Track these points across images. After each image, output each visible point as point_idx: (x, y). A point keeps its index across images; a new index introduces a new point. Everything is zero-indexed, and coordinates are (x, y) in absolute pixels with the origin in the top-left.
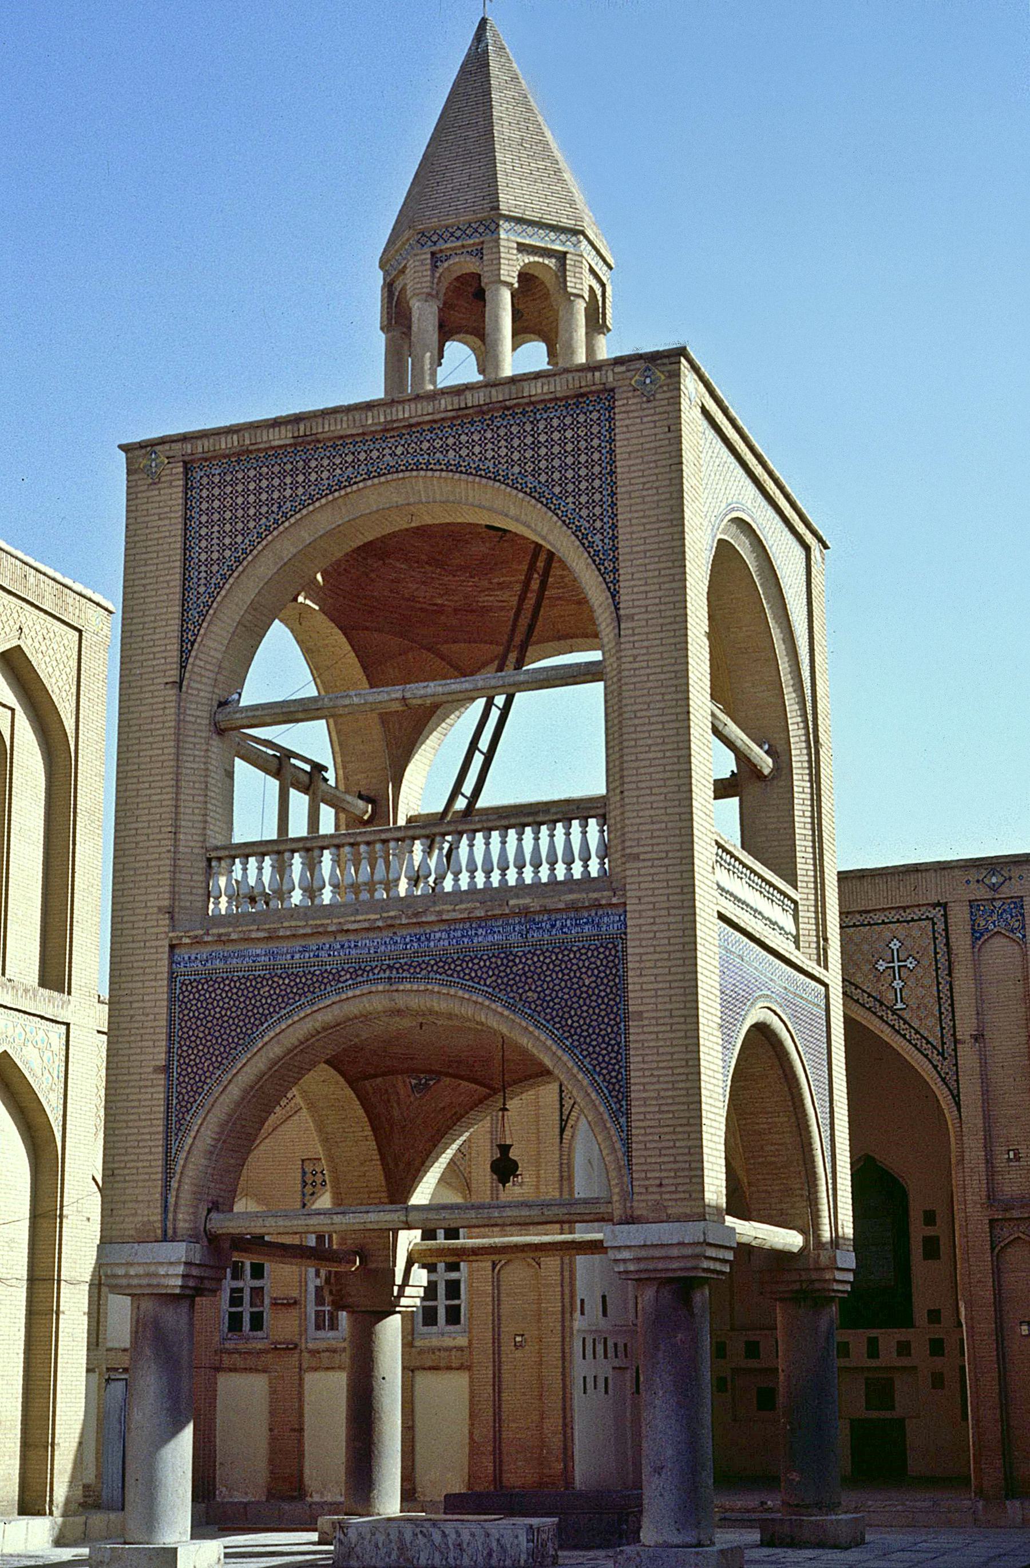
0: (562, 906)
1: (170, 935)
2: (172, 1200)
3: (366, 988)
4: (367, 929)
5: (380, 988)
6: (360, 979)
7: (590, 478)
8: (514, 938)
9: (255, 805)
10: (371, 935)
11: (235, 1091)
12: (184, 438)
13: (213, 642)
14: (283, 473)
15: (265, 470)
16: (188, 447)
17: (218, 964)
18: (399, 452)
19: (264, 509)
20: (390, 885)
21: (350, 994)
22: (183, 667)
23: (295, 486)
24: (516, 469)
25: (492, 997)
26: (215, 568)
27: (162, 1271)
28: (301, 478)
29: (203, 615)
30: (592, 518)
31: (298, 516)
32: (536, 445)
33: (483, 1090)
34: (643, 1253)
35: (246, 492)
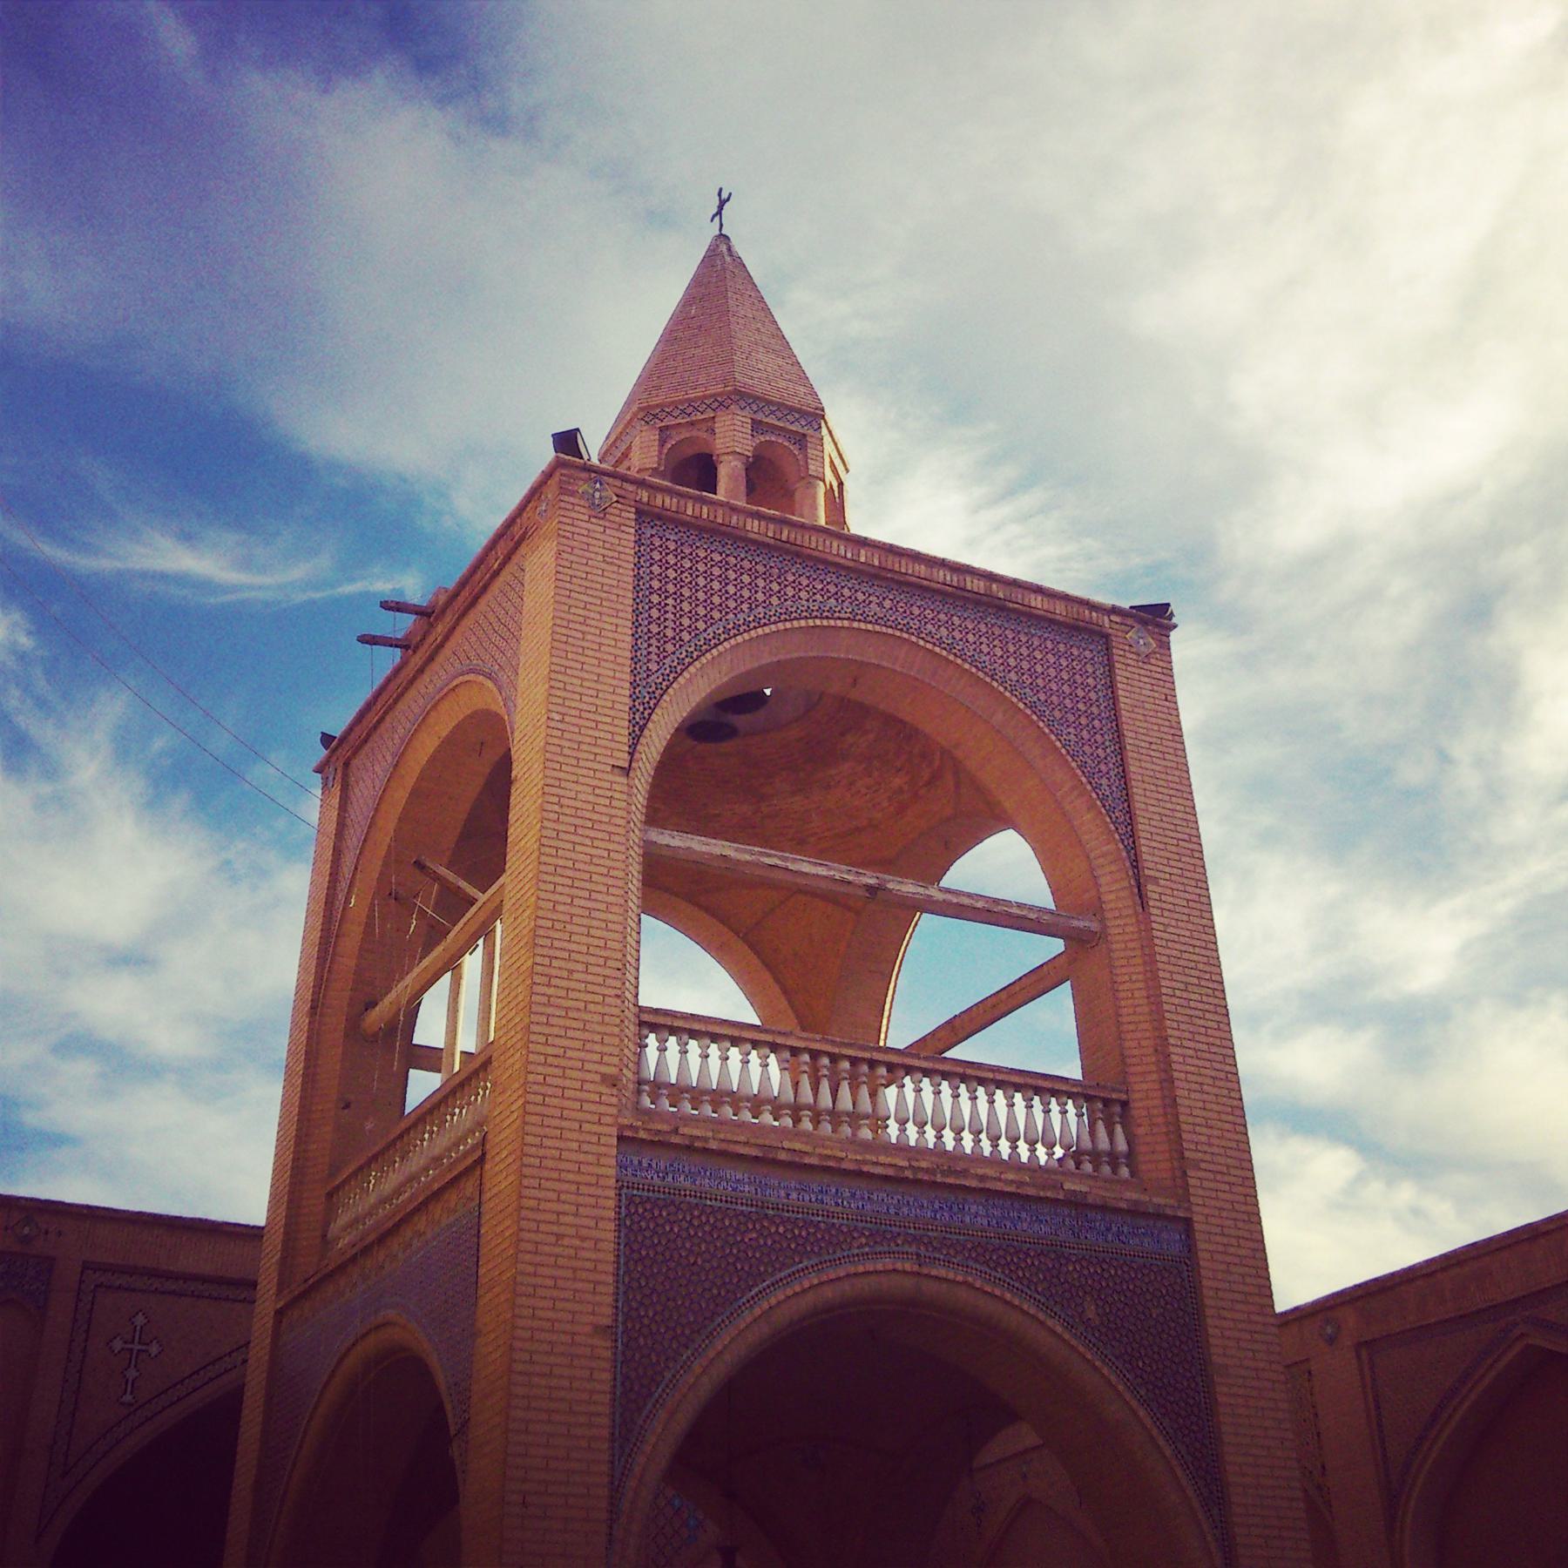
0: (1123, 1205)
1: (621, 1120)
4: (886, 1178)
5: (908, 1267)
6: (879, 1249)
10: (889, 1187)
15: (732, 560)
17: (683, 1182)
28: (775, 587)
31: (905, 636)
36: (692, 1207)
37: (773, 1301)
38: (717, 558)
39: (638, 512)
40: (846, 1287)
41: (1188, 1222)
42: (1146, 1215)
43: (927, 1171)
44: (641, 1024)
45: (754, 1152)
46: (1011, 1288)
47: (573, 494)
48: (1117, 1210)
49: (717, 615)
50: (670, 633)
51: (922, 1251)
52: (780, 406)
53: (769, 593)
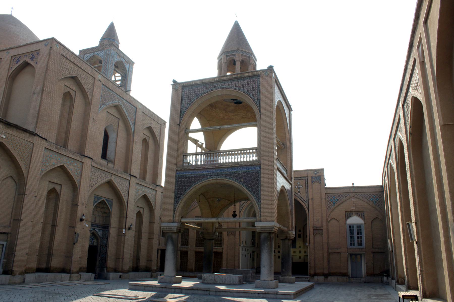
3: (212, 179)
7: (255, 90)
9: (191, 148)
11: (187, 196)
13: (186, 118)
14: (199, 89)
20: (218, 160)
22: (180, 122)
25: (235, 181)
29: (184, 113)
30: (256, 97)
35: (193, 92)
40: (206, 183)
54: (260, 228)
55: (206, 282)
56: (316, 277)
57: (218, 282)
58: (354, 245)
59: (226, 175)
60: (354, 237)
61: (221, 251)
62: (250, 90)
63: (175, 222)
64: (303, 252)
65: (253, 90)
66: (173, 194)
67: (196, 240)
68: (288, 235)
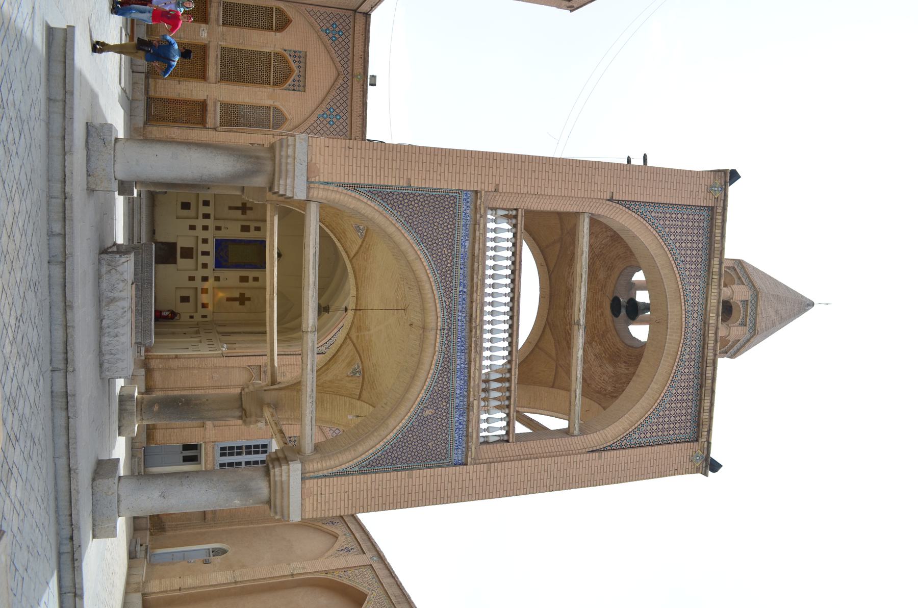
0: (470, 430)
2: (331, 187)
3: (440, 315)
4: (471, 316)
5: (439, 324)
8: (456, 402)
12: (725, 208)
15: (700, 253)
16: (719, 210)
17: (463, 221)
18: (694, 329)
19: (683, 252)
21: (438, 305)
22: (618, 202)
23: (690, 270)
24: (674, 391)
26: (661, 222)
27: (289, 181)
28: (693, 274)
32: (682, 401)
33: (352, 254)
34: (285, 486)
36: (454, 224)
37: (423, 260)
38: (700, 245)
39: (712, 208)
41: (466, 464)
42: (467, 442)
43: (476, 334)
44: (516, 209)
45: (476, 252)
46: (435, 373)
47: (715, 178)
48: (468, 428)
49: (678, 245)
50: (667, 223)
51: (446, 332)
52: (756, 313)
53: (690, 270)
54: (284, 478)
55: (104, 269)
56: (142, 372)
57: (105, 313)
58: (222, 455)
59: (447, 360)
60: (239, 454)
61: (210, 122)
62: (665, 416)
63: (309, 188)
64: (206, 222)
65: (663, 423)
66: (403, 183)
67: (240, 51)
68: (253, 419)
